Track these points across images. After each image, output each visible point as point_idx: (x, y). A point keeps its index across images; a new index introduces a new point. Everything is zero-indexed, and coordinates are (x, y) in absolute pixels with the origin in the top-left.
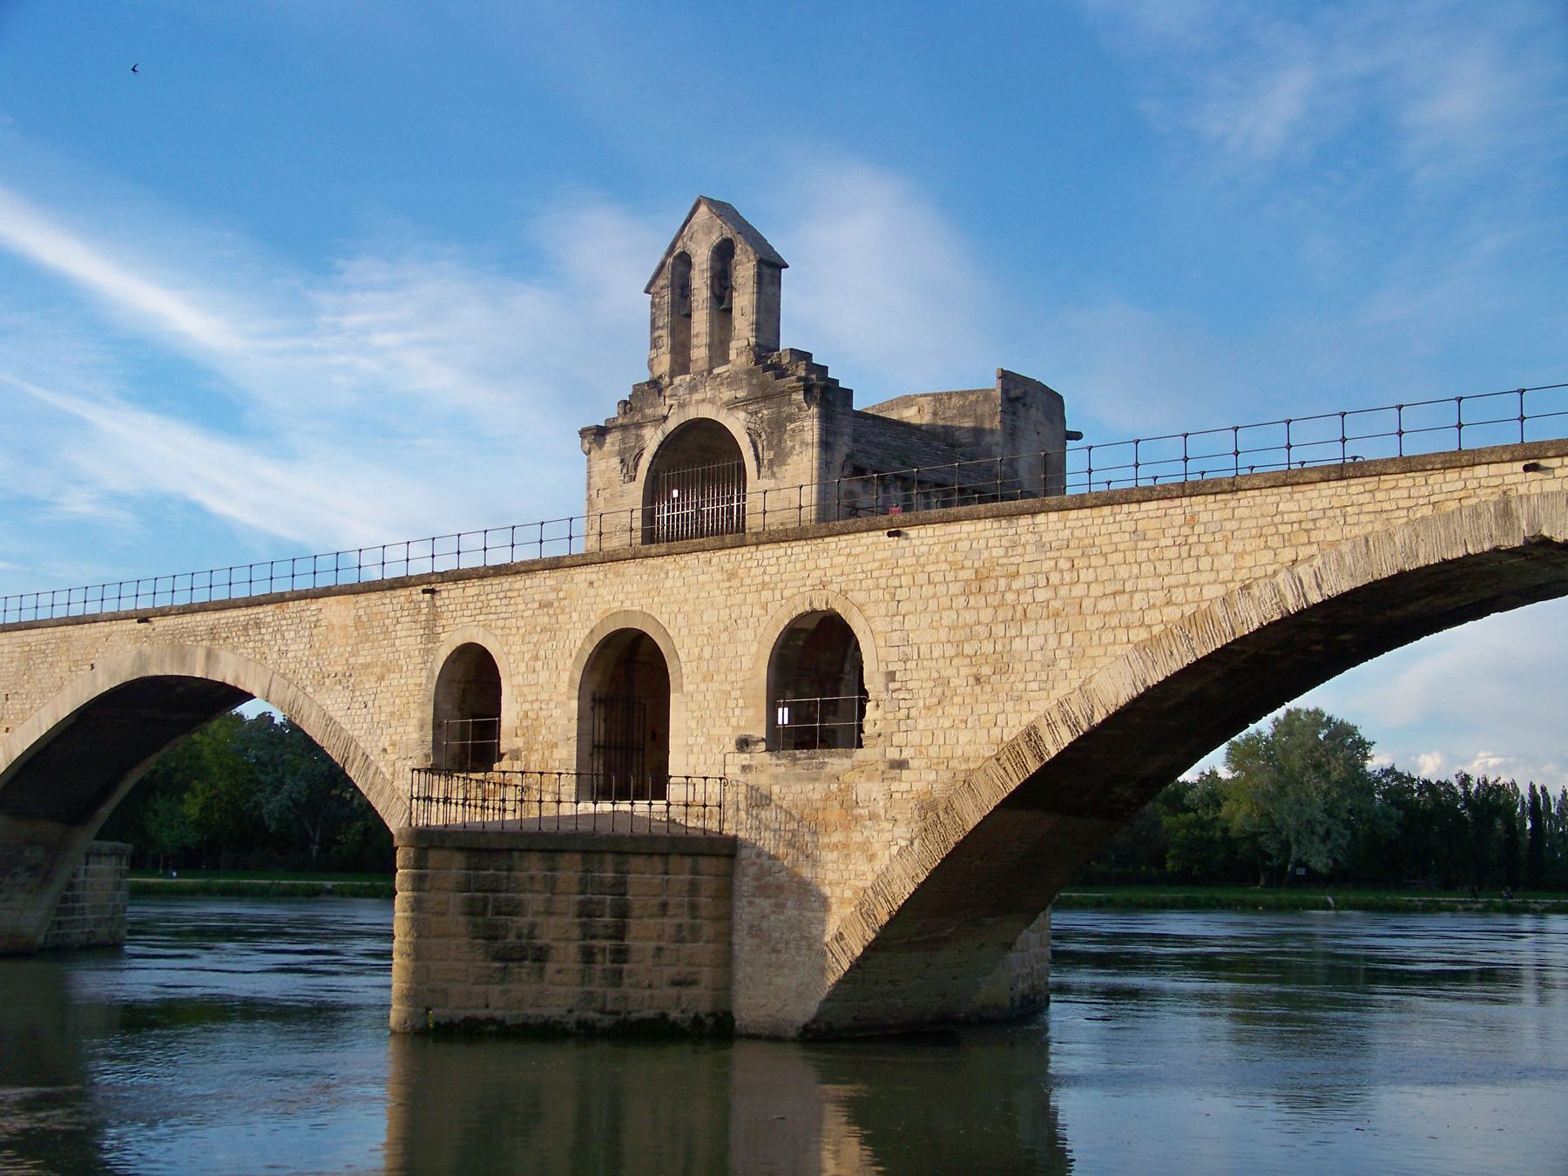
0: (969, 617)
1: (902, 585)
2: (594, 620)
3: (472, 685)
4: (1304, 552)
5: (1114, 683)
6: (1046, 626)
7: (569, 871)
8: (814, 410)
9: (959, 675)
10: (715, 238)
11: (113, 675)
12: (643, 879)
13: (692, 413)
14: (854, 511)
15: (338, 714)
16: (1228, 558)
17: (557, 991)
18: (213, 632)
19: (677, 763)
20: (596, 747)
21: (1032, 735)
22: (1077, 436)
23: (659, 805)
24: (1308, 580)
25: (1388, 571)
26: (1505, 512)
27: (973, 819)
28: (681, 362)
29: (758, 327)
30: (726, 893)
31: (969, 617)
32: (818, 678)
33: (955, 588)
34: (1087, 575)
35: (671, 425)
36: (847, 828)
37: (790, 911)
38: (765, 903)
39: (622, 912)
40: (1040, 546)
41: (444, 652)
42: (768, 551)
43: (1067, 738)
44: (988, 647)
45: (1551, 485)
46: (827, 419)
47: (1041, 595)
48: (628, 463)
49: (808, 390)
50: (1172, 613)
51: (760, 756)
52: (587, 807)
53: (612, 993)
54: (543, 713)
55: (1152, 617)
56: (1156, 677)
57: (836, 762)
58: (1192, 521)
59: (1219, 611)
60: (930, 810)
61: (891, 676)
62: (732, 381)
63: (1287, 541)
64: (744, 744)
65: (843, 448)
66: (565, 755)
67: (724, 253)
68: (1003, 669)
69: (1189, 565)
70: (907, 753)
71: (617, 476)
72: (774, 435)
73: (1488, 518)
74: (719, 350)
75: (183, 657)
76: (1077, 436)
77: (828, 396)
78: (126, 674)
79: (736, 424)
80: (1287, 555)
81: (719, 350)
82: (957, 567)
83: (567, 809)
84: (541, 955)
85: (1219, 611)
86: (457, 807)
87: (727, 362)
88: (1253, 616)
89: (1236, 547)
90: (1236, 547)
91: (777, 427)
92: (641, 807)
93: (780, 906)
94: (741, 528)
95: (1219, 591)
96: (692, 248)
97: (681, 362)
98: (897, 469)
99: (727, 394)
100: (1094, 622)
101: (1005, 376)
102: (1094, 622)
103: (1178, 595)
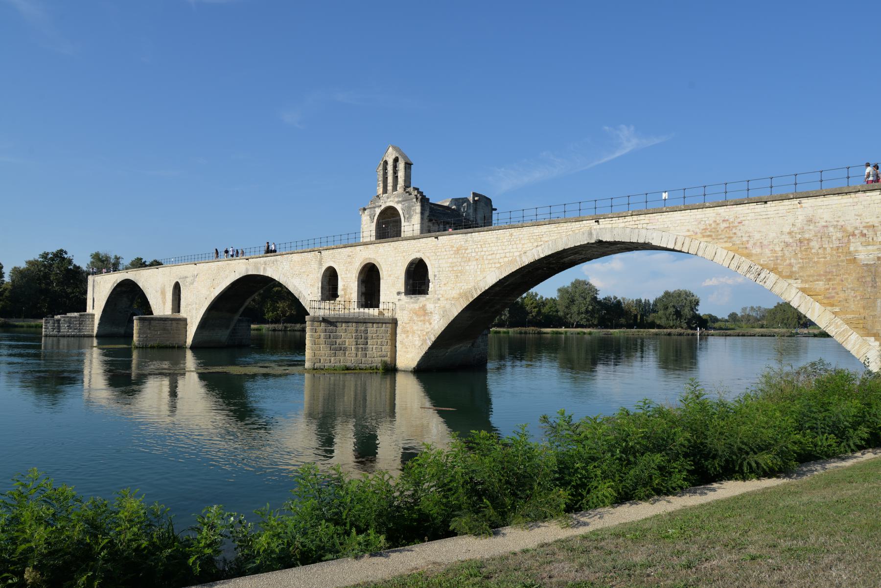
0: (455, 260)
1: (442, 252)
3: (330, 279)
4: (540, 243)
5: (491, 278)
6: (475, 263)
7: (352, 327)
8: (419, 204)
10: (394, 157)
12: (372, 329)
13: (388, 204)
14: (429, 232)
15: (297, 285)
17: (350, 358)
18: (265, 263)
19: (382, 300)
20: (363, 294)
22: (495, 210)
23: (376, 310)
24: (540, 251)
25: (560, 249)
26: (590, 234)
28: (385, 191)
29: (405, 181)
30: (394, 334)
31: (455, 260)
32: (417, 278)
33: (452, 252)
34: (485, 249)
35: (382, 208)
36: (424, 315)
37: (410, 337)
38: (404, 336)
39: (366, 338)
40: (473, 241)
41: (324, 269)
42: (405, 242)
43: (479, 293)
44: (460, 268)
45: (601, 226)
46: (422, 206)
47: (473, 254)
48: (372, 217)
49: (417, 199)
50: (506, 259)
51: (403, 296)
52: (362, 310)
53: (363, 359)
54: (349, 285)
55: (501, 260)
57: (422, 299)
58: (511, 235)
59: (518, 259)
61: (435, 276)
62: (398, 196)
63: (536, 240)
64: (399, 293)
65: (427, 213)
67: (396, 160)
69: (510, 247)
70: (440, 296)
71: (369, 221)
72: (409, 211)
73: (586, 235)
74: (395, 188)
75: (258, 269)
76: (495, 210)
77: (424, 201)
78: (243, 274)
79: (399, 207)
80: (536, 244)
81: (395, 188)
82: (452, 247)
83: (357, 310)
84: (345, 349)
85: (518, 259)
86: (326, 309)
87: (396, 190)
88: (527, 260)
89: (523, 242)
90: (523, 242)
93: (408, 336)
95: (518, 254)
96: (387, 159)
98: (441, 219)
99: (396, 199)
100: (486, 262)
101: (475, 195)
102: (486, 262)
103: (508, 255)
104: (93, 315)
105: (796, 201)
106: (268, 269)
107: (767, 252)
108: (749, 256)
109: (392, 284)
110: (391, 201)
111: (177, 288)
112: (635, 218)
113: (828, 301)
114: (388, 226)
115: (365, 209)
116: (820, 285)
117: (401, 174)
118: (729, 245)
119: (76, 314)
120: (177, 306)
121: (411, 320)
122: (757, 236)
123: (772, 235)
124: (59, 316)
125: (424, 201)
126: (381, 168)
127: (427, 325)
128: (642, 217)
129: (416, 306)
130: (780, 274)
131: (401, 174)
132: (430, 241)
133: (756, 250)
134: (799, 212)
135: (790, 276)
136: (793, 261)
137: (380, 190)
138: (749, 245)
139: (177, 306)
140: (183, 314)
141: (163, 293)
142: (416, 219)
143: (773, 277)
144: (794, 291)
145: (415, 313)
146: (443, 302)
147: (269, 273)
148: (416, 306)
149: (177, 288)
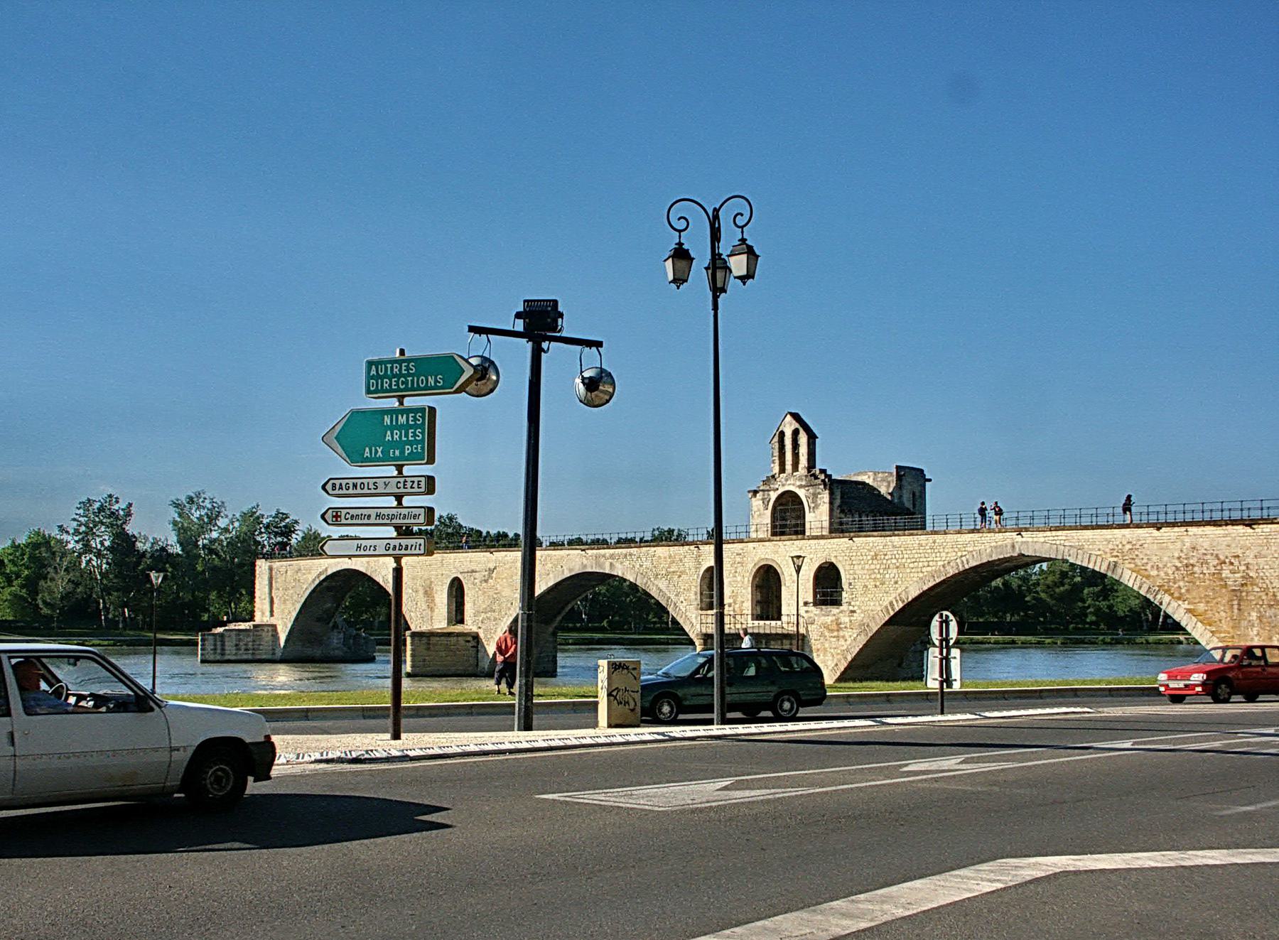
2: (756, 559)
3: (713, 580)
9: (871, 584)
11: (570, 570)
13: (787, 488)
16: (943, 554)
18: (612, 556)
19: (784, 610)
21: (891, 603)
23: (779, 623)
26: (1013, 546)
27: (875, 629)
28: (782, 470)
32: (828, 585)
35: (779, 492)
43: (901, 605)
46: (831, 494)
48: (765, 502)
49: (825, 485)
51: (811, 608)
56: (925, 588)
57: (834, 610)
60: (863, 626)
62: (800, 479)
65: (838, 502)
66: (747, 607)
68: (883, 584)
71: (762, 508)
75: (601, 566)
79: (802, 493)
88: (951, 572)
91: (815, 495)
92: (773, 623)
94: (803, 532)
97: (782, 470)
104: (274, 627)
105: (1183, 529)
106: (618, 565)
107: (1162, 574)
108: (1148, 577)
109: (796, 592)
110: (793, 483)
111: (457, 589)
112: (1054, 533)
113: (1208, 623)
114: (787, 518)
115: (755, 492)
116: (1201, 607)
117: (803, 450)
118: (1132, 566)
119: (243, 626)
120: (457, 613)
121: (822, 635)
122: (1154, 558)
123: (1165, 559)
124: (220, 630)
125: (832, 485)
126: (776, 439)
127: (842, 642)
128: (1060, 533)
129: (829, 619)
130: (1172, 595)
131: (803, 450)
132: (843, 542)
133: (1154, 573)
134: (1186, 539)
135: (1179, 598)
136: (1181, 584)
137: (776, 469)
138: (1148, 567)
139: (457, 613)
140: (470, 625)
141: (429, 593)
142: (824, 508)
143: (1167, 598)
144: (1182, 611)
145: (827, 628)
146: (858, 617)
147: (618, 572)
148: (829, 619)
149: (457, 589)
